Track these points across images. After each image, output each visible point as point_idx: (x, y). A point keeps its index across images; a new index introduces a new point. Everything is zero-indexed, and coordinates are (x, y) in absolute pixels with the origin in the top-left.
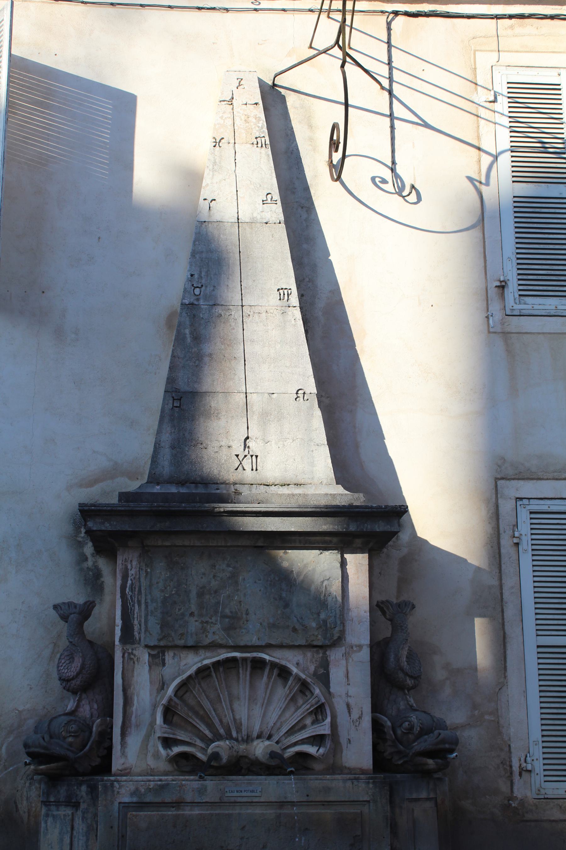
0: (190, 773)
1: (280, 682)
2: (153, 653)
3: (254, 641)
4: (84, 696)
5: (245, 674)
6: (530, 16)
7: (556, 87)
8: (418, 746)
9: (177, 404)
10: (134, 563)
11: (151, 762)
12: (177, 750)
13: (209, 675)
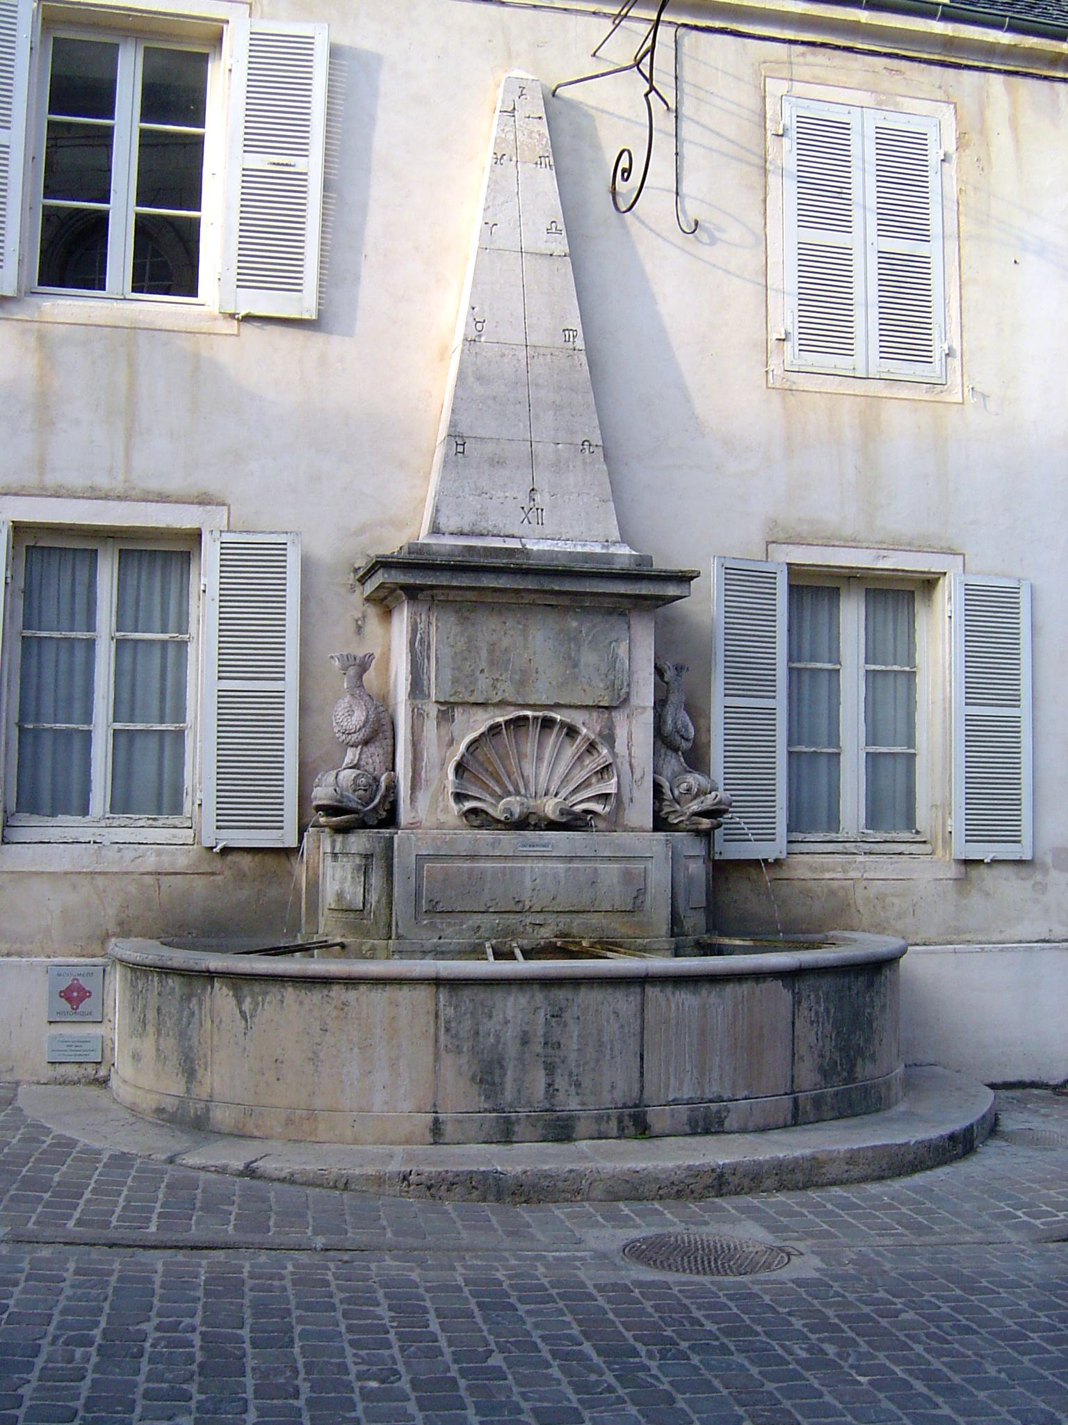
0: (480, 827)
1: (568, 740)
2: (443, 708)
3: (544, 700)
4: (365, 749)
5: (534, 731)
6: (823, 45)
7: (845, 126)
8: (695, 806)
9: (460, 449)
10: (423, 617)
11: (443, 818)
12: (468, 805)
13: (500, 733)
